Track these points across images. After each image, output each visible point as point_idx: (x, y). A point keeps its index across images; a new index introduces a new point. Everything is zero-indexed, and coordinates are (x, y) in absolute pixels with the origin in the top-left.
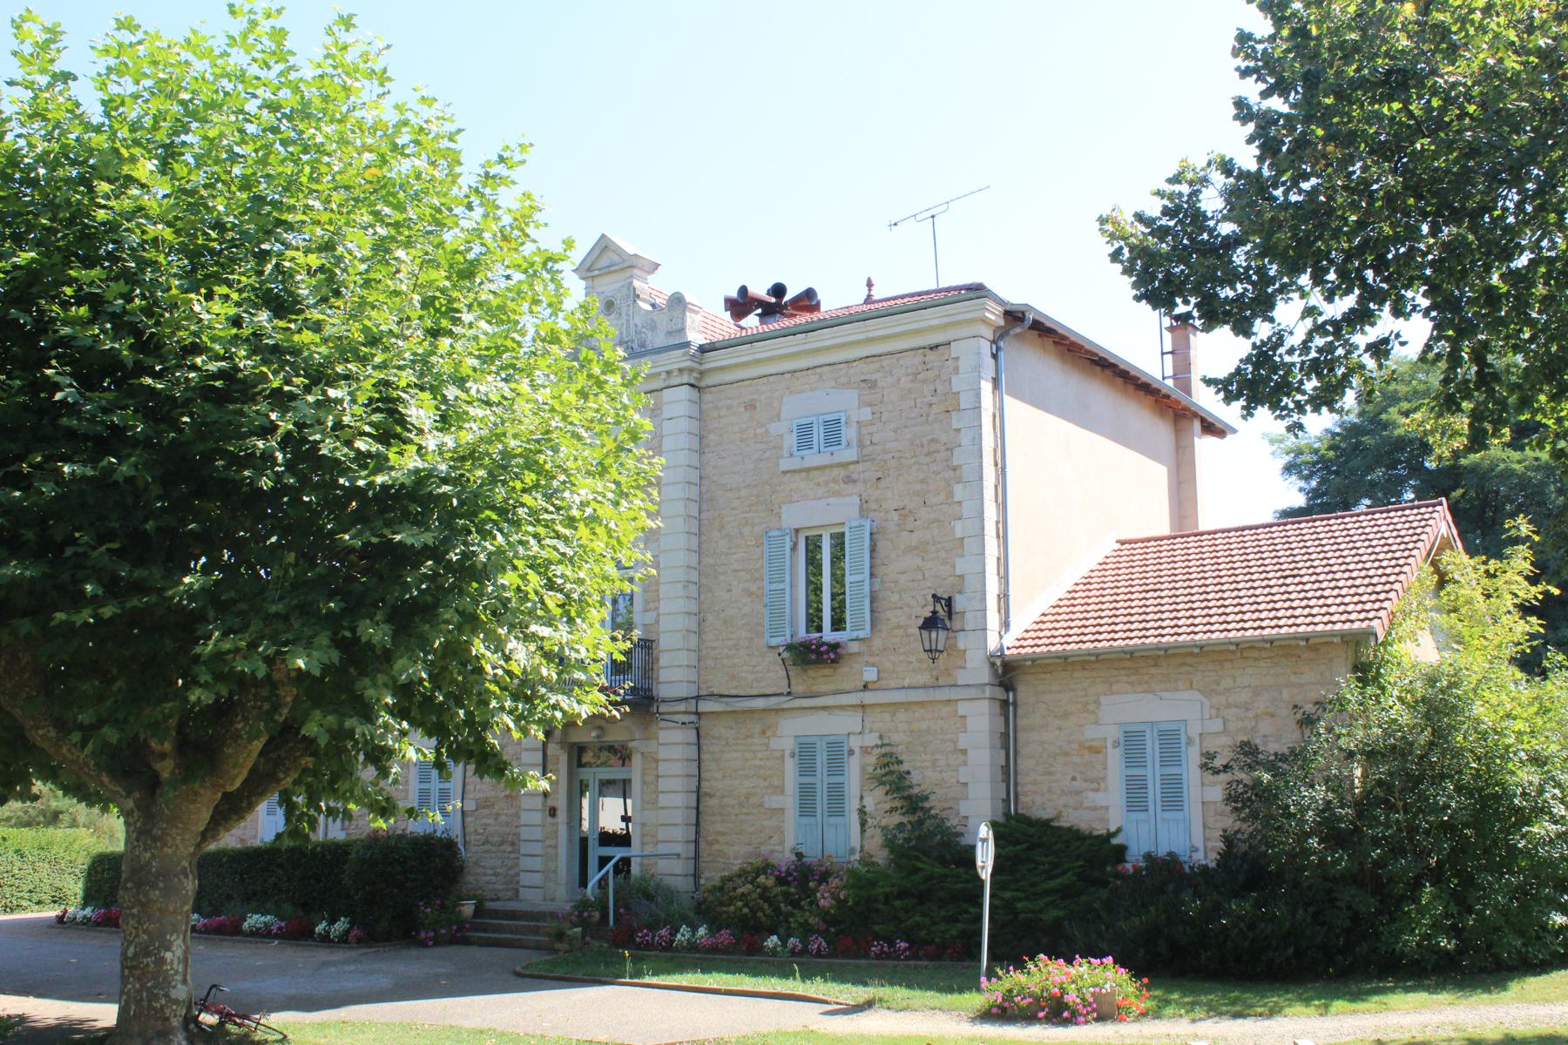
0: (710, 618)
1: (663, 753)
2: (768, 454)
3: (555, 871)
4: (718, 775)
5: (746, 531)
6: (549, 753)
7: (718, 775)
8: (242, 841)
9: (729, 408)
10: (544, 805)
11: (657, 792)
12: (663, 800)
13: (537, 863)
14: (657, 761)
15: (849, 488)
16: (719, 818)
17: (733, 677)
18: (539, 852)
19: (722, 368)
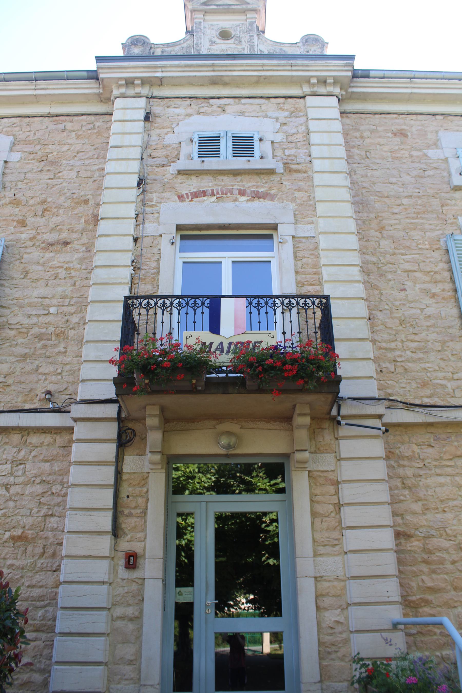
0: (380, 316)
1: (347, 471)
2: (431, 173)
3: (135, 662)
4: (417, 507)
5: (416, 235)
6: (126, 468)
7: (417, 507)
9: (372, 132)
10: (115, 548)
11: (341, 528)
12: (353, 540)
13: (97, 649)
14: (337, 483)
16: (425, 568)
17: (424, 385)
18: (102, 627)
19: (364, 97)
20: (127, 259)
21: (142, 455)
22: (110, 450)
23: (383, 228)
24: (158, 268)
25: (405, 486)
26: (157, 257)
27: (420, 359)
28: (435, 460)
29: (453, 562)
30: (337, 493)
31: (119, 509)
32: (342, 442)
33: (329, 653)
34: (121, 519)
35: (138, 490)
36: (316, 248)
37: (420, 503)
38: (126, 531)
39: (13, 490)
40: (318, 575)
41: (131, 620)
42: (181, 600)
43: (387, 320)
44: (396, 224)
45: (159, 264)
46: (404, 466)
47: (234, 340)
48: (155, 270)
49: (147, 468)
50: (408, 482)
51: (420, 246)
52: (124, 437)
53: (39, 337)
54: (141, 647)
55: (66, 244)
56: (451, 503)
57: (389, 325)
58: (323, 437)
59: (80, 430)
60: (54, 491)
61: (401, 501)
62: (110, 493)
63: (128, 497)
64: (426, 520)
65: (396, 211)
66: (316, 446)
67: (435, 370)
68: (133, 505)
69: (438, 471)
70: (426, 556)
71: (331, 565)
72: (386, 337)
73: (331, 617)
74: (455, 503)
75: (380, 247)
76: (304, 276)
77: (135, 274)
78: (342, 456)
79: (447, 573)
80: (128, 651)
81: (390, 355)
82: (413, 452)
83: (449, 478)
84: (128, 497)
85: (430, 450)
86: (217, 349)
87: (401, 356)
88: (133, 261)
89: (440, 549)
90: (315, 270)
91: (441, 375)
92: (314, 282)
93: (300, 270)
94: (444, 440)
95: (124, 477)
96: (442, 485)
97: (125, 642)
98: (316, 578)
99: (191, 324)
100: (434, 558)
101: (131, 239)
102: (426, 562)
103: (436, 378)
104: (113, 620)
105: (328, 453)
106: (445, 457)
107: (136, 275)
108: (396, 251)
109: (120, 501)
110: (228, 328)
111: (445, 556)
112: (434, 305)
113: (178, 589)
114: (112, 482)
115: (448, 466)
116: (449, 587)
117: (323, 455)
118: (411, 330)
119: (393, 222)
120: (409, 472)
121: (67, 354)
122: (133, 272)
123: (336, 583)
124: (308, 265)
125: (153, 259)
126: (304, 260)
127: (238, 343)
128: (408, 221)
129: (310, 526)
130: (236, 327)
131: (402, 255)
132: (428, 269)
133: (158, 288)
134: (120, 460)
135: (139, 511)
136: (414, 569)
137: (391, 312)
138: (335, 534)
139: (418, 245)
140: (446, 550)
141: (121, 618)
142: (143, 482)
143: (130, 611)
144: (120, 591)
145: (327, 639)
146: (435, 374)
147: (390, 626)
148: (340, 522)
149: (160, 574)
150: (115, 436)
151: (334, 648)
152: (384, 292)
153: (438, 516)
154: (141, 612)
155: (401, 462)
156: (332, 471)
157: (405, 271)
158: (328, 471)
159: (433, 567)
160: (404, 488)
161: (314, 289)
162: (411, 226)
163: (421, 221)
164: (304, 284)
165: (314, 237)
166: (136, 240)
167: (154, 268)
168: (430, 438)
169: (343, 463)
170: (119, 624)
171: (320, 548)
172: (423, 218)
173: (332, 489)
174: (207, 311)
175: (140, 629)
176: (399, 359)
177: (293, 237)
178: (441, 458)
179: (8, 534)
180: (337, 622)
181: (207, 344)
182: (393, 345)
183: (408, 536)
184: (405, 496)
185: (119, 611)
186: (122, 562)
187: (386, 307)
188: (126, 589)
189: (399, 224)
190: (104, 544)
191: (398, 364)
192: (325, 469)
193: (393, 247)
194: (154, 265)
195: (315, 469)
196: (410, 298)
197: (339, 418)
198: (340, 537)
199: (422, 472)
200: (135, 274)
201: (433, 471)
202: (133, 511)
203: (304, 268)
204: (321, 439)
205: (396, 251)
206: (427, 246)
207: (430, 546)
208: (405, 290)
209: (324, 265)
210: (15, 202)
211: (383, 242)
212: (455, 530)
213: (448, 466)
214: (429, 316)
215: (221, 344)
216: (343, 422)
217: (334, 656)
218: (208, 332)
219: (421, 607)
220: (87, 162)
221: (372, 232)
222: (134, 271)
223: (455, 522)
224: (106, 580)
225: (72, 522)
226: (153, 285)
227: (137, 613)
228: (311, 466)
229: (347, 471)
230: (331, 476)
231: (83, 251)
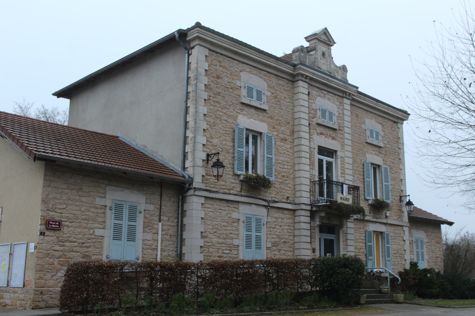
8: (85, 256)
15: (380, 154)
32: (348, 223)
39: (283, 227)
53: (283, 176)
55: (286, 140)
150: (309, 215)
173: (345, 235)
179: (282, 241)
210: (272, 118)
220: (288, 104)
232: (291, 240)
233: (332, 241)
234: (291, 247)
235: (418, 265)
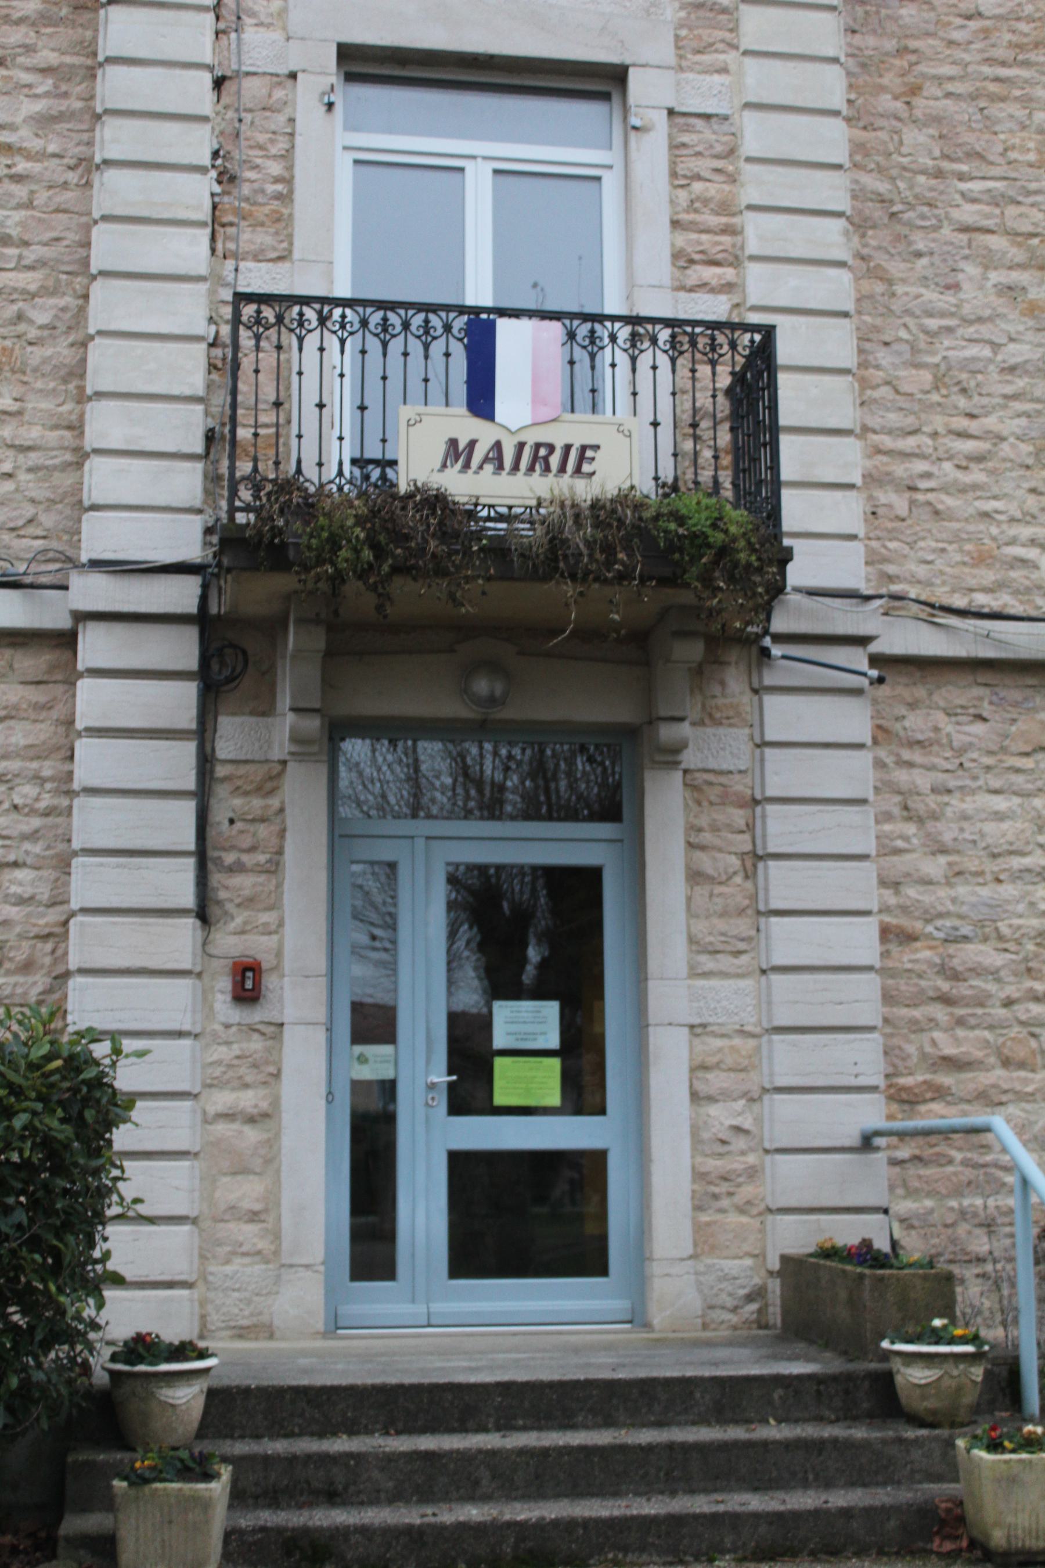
4: (935, 867)
6: (224, 749)
16: (940, 1013)
20: (197, 144)
21: (263, 714)
22: (180, 702)
23: (915, 90)
24: (288, 181)
25: (909, 814)
26: (282, 145)
27: (975, 487)
28: (990, 753)
29: (1008, 1003)
30: (750, 827)
31: (212, 853)
32: (772, 702)
33: (715, 1197)
34: (216, 878)
35: (257, 803)
36: (731, 152)
37: (942, 860)
38: (230, 907)
40: (697, 1021)
41: (251, 1120)
42: (365, 1073)
43: (902, 373)
44: (951, 79)
45: (290, 168)
46: (910, 765)
47: (531, 438)
48: (279, 187)
49: (280, 746)
50: (915, 803)
51: (1013, 155)
52: (215, 666)
54: (277, 1181)
56: (1017, 862)
57: (905, 388)
58: (723, 684)
59: (95, 647)
60: (18, 801)
61: (898, 851)
62: (188, 809)
63: (232, 821)
64: (954, 900)
65: (957, 35)
66: (704, 706)
67: (1013, 520)
68: (246, 842)
69: (996, 783)
70: (945, 986)
71: (732, 999)
72: (894, 419)
73: (721, 1116)
74: (1027, 861)
75: (905, 150)
76: (694, 236)
77: (225, 193)
78: (769, 736)
79: (991, 1027)
80: (247, 1192)
81: (900, 469)
82: (936, 729)
83: (1016, 800)
84: (232, 821)
85: (979, 728)
86: (486, 460)
87: (927, 475)
88: (216, 154)
89: (978, 971)
90: (724, 220)
91: (1026, 532)
92: (720, 256)
93: (684, 217)
94: (1016, 704)
95: (221, 771)
96: (999, 817)
97: (241, 1170)
98: (692, 1027)
99: (415, 385)
100: (963, 990)
101: (207, 79)
102: (946, 1000)
103: (1013, 542)
104: (206, 1121)
105: (731, 725)
106: (1014, 748)
107: (226, 199)
108: (946, 165)
109: (211, 833)
110: (515, 404)
111: (992, 987)
112: (1029, 336)
113: (358, 1049)
114: (190, 783)
115: (1018, 771)
116: (992, 1060)
117: (721, 731)
118: (962, 402)
119: (947, 70)
120: (923, 780)
121: (26, 418)
122: (217, 189)
123: (737, 1041)
124: (706, 202)
125: (274, 151)
126: (697, 186)
127: (538, 446)
128: (986, 70)
129: (684, 907)
130: (537, 400)
131: (962, 177)
132: (1026, 227)
133: (291, 244)
134: (209, 726)
135: (261, 858)
136: (916, 1013)
137: (914, 350)
138: (743, 926)
139: (1006, 150)
140: (994, 974)
141: (228, 1116)
142: (269, 786)
143: (248, 1100)
144: (221, 1053)
145: (712, 1165)
146: (1013, 531)
147: (855, 1141)
148: (754, 898)
149: (320, 1014)
150: (191, 661)
151: (723, 1188)
152: (899, 289)
153: (985, 892)
154: (276, 1102)
155: (906, 755)
156: (740, 772)
157: (965, 229)
158: (731, 772)
159: (961, 1012)
160: (909, 819)
161: (720, 277)
162: (993, 87)
163: (1025, 73)
164: (692, 262)
165: (726, 118)
166: (219, 83)
167: (277, 180)
168: (981, 699)
169: (768, 752)
170: (222, 1128)
171: (703, 958)
172: (1026, 64)
173: (738, 816)
174: (458, 350)
175: (272, 1143)
176: (923, 484)
177: (671, 112)
178: (1004, 750)
180: (738, 1129)
181: (461, 446)
182: (909, 443)
183: (909, 938)
184: (906, 839)
185: (221, 1100)
186: (225, 983)
187: (903, 334)
188: (236, 1050)
189: (962, 78)
190: (179, 941)
191: (920, 497)
192: (725, 767)
193: (937, 153)
194: (275, 168)
195: (700, 766)
196: (966, 309)
197: (767, 641)
198: (753, 933)
199: (952, 783)
200: (225, 193)
201: (981, 782)
202: (245, 858)
203: (696, 211)
204: (717, 690)
205: (946, 165)
206: (1032, 157)
207: (956, 963)
208: (956, 287)
209: (750, 207)
211: (914, 137)
212: (1019, 927)
213: (1018, 771)
214: (1012, 369)
215: (498, 445)
216: (776, 651)
217: (725, 1203)
218: (463, 410)
219: (925, 1101)
221: (886, 102)
222: (220, 182)
223: (1021, 908)
224: (187, 1027)
225: (90, 883)
226: (277, 233)
227: (264, 1105)
228: (690, 758)
229: (782, 774)
230: (740, 786)
231: (47, 94)
232: (21, 901)
233: (589, 879)
234: (27, 967)
235: (122, 1126)
